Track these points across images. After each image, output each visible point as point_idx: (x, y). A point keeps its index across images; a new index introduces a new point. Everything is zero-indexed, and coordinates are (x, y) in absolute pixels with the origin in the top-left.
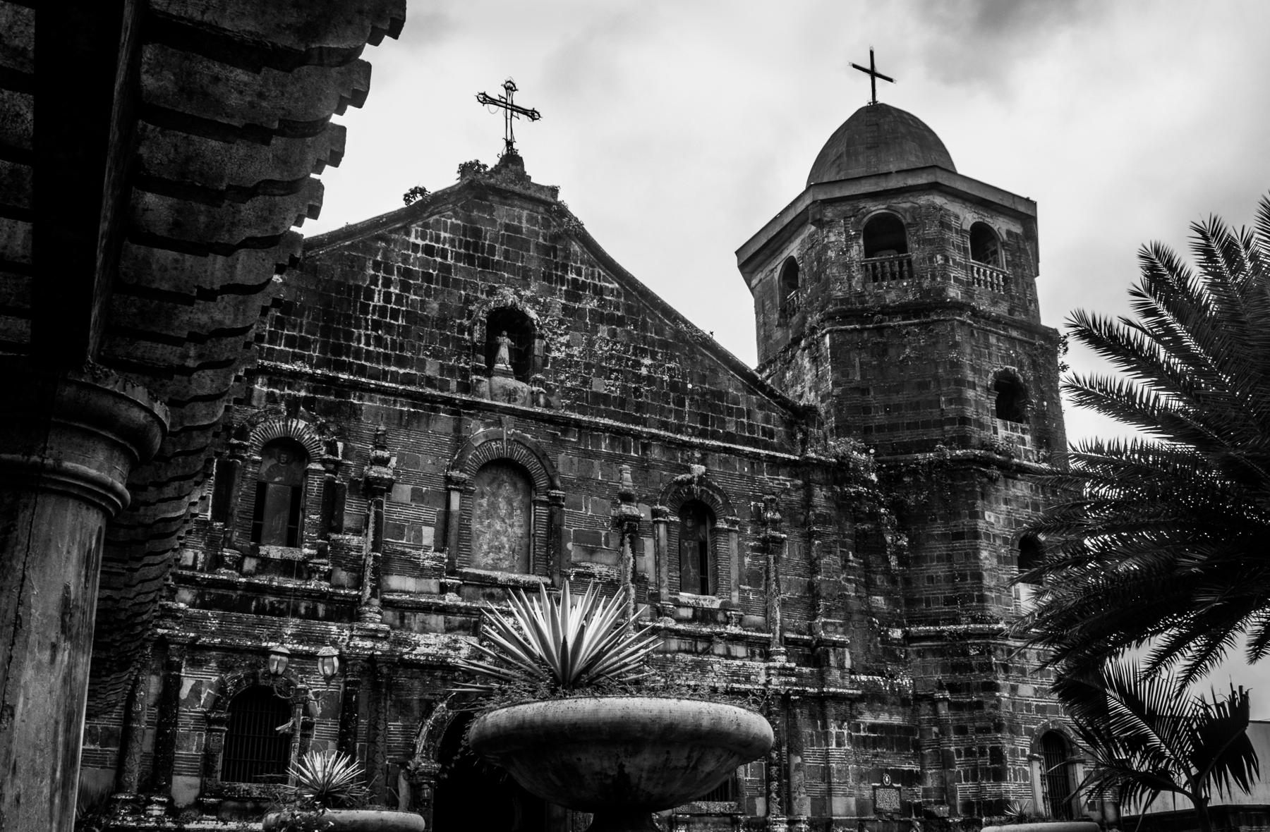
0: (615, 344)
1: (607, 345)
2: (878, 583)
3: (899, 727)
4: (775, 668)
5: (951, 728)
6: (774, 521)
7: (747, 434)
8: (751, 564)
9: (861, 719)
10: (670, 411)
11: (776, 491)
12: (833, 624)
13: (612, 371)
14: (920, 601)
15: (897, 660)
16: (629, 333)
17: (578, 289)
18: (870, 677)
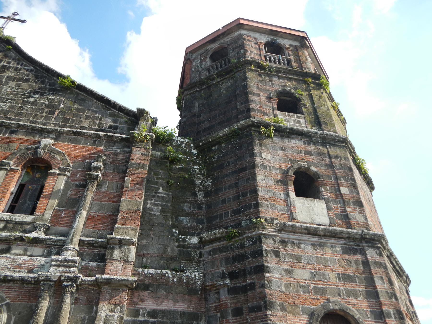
0: (18, 89)
1: (12, 89)
2: (185, 208)
3: (183, 314)
4: (57, 261)
5: (230, 311)
6: (97, 169)
7: (96, 127)
8: (71, 195)
9: (142, 305)
10: (42, 116)
11: (107, 154)
12: (127, 229)
13: (7, 99)
14: (216, 217)
15: (189, 259)
16: (30, 85)
17: (4, 69)
18: (159, 271)
